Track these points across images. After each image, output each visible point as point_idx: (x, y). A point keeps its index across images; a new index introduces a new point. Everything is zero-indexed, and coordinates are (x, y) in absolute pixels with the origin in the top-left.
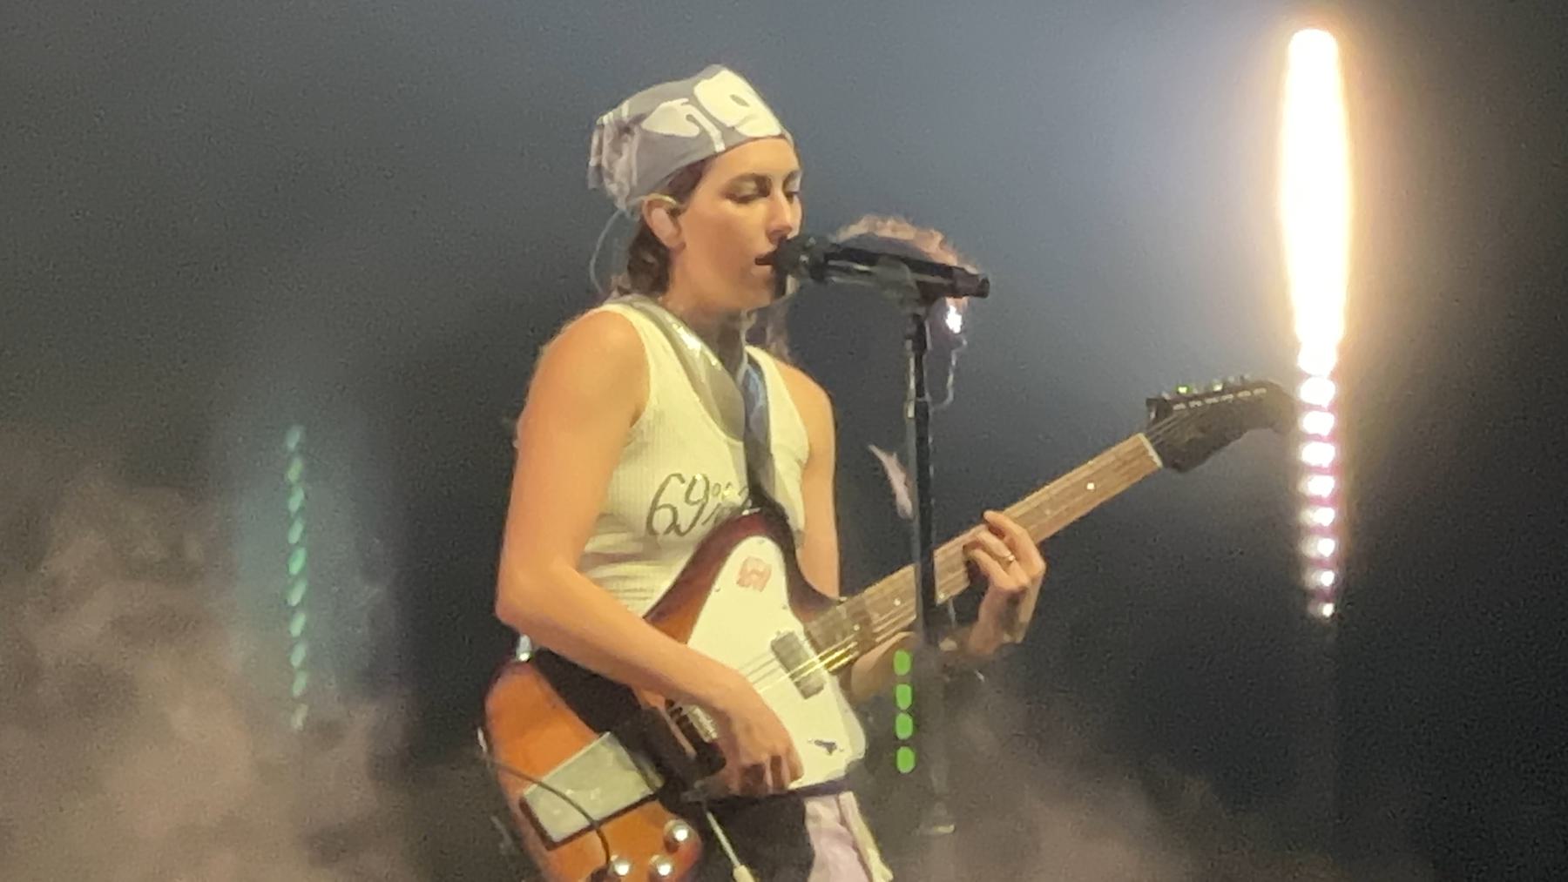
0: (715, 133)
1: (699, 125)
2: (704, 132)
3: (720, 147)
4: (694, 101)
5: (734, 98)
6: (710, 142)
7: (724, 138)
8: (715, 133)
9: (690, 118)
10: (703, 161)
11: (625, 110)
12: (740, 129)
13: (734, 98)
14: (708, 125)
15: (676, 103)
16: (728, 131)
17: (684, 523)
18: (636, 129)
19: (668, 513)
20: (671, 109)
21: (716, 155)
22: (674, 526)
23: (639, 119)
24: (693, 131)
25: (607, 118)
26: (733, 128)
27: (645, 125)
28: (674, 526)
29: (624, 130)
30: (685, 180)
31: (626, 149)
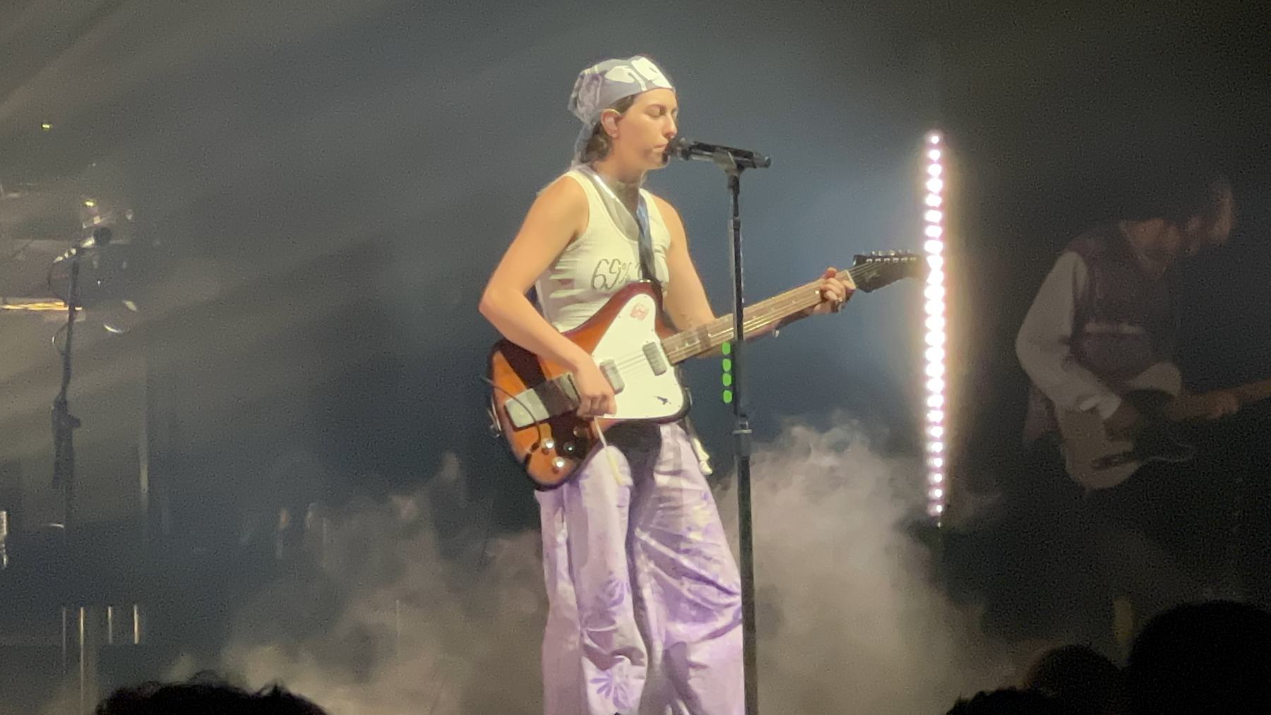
0: (642, 82)
2: (637, 84)
3: (644, 89)
8: (642, 82)
9: (630, 74)
11: (596, 69)
14: (639, 78)
15: (623, 67)
16: (649, 82)
17: (610, 282)
19: (601, 278)
22: (605, 285)
23: (603, 73)
24: (632, 80)
25: (587, 71)
28: (605, 285)
29: (595, 77)
30: (624, 105)
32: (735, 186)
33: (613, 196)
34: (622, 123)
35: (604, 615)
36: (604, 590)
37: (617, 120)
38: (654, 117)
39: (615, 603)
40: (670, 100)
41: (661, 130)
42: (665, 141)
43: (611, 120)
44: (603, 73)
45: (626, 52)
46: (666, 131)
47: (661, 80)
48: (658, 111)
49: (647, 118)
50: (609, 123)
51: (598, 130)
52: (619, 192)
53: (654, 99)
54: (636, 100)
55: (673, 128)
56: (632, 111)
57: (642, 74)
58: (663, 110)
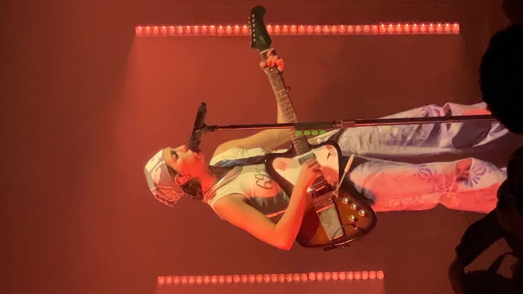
3: (164, 162)
6: (162, 164)
7: (162, 161)
9: (156, 170)
10: (168, 167)
11: (153, 189)
14: (158, 166)
15: (152, 174)
18: (158, 186)
20: (154, 175)
21: (166, 163)
24: (160, 169)
27: (157, 183)
29: (158, 189)
31: (163, 191)
32: (213, 128)
33: (222, 180)
35: (435, 179)
36: (424, 179)
38: (177, 156)
39: (431, 175)
40: (168, 150)
41: (184, 154)
42: (190, 152)
44: (156, 185)
46: (185, 150)
47: (160, 154)
48: (174, 156)
49: (179, 161)
50: (183, 181)
51: (185, 187)
52: (219, 178)
54: (169, 165)
56: (175, 168)
57: (154, 167)
58: (174, 153)
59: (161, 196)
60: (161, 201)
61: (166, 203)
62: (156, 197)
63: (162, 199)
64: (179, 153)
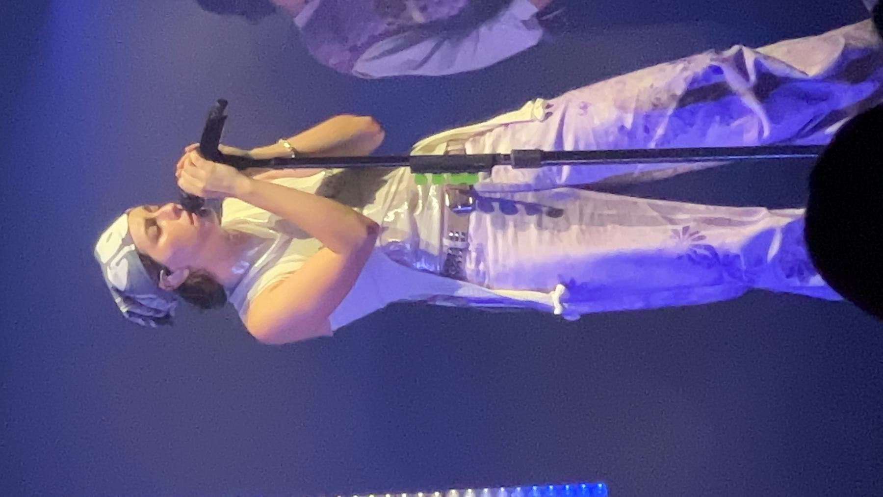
0: (126, 249)
1: (121, 259)
3: (133, 247)
4: (108, 263)
5: (108, 241)
6: (130, 252)
7: (129, 244)
8: (126, 249)
9: (118, 264)
11: (118, 300)
12: (124, 235)
13: (108, 241)
18: (127, 294)
20: (116, 276)
24: (125, 263)
26: (123, 240)
34: (172, 269)
37: (168, 273)
43: (170, 278)
45: (95, 268)
48: (153, 230)
49: (163, 240)
50: (174, 281)
53: (140, 232)
55: (169, 207)
59: (138, 311)
60: (140, 321)
61: (153, 324)
62: (127, 316)
63: (140, 316)
64: (163, 223)
